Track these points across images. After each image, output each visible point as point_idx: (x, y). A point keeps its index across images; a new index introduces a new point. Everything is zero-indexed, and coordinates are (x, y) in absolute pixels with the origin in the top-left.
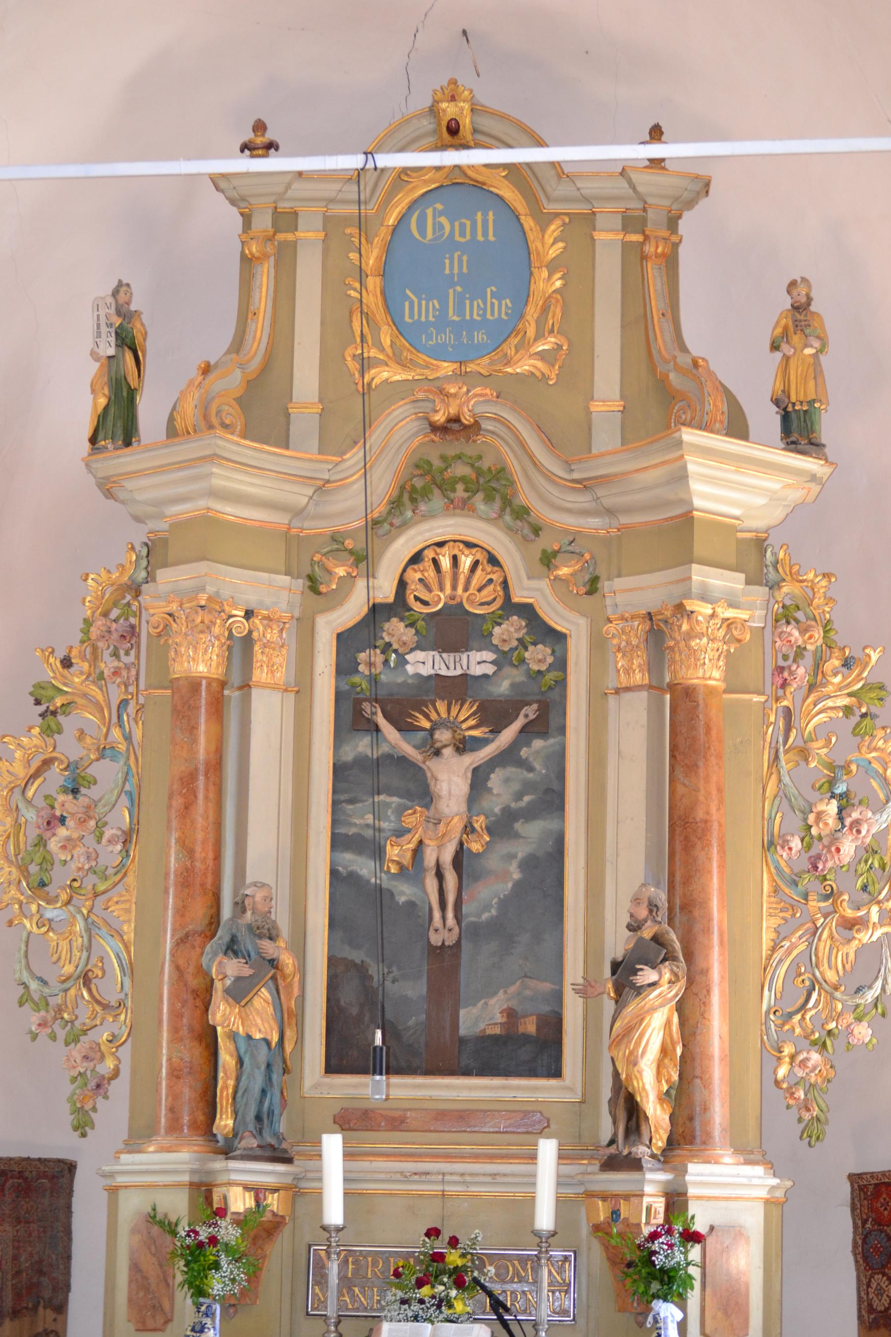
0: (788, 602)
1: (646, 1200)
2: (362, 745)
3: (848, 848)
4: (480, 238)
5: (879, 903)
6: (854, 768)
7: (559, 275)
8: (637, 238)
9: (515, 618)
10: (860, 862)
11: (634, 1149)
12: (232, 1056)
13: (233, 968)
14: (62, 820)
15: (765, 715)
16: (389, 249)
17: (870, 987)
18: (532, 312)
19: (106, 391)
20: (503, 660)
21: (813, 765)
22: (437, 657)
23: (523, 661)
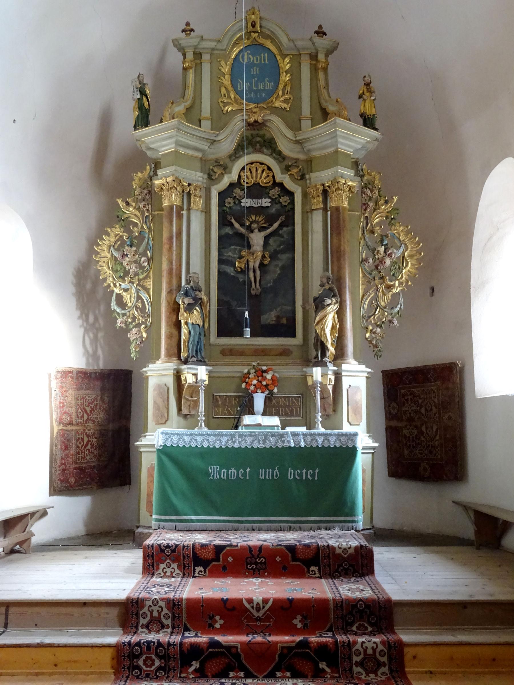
0: (366, 182)
1: (329, 377)
2: (228, 230)
3: (388, 261)
4: (263, 62)
5: (398, 280)
6: (389, 235)
7: (289, 75)
8: (314, 62)
9: (277, 188)
10: (392, 266)
11: (324, 359)
12: (187, 330)
13: (187, 301)
14: (127, 255)
15: (360, 219)
16: (233, 66)
17: (396, 307)
18: (281, 87)
19: (137, 110)
20: (274, 201)
21: (376, 235)
22: (251, 201)
23: (280, 202)
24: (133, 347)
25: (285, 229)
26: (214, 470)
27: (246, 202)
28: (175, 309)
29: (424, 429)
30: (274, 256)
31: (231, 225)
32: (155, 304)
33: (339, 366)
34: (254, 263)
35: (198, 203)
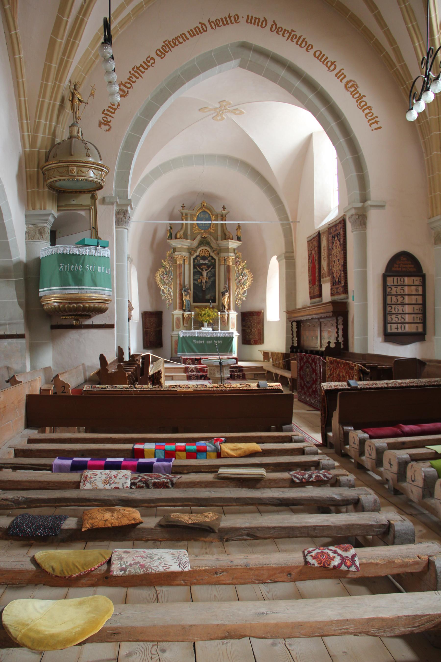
2: (195, 270)
3: (243, 281)
13: (185, 293)
20: (209, 261)
25: (213, 270)
28: (181, 295)
29: (252, 330)
30: (209, 278)
31: (197, 268)
32: (175, 293)
33: (229, 312)
34: (204, 281)
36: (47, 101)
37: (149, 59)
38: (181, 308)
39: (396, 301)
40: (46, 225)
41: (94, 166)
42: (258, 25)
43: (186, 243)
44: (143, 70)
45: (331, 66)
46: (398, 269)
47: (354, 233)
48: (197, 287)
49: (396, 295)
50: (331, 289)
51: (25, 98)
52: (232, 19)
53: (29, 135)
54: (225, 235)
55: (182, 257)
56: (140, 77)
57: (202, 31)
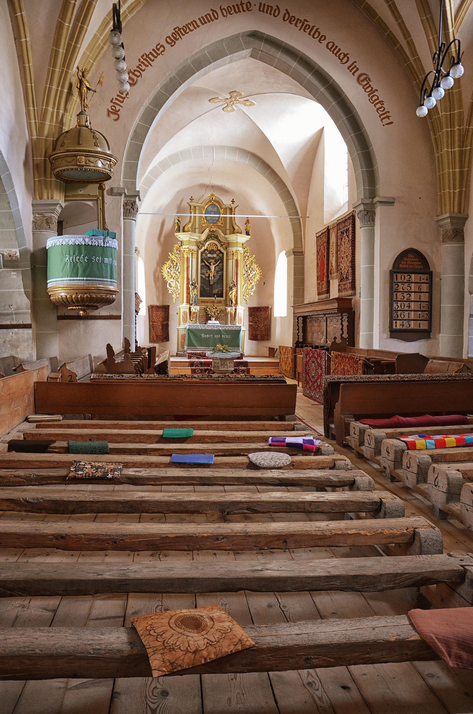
2: (203, 264)
3: (251, 275)
24: (174, 299)
26: (203, 335)
27: (209, 255)
28: (188, 288)
30: (217, 272)
31: (204, 262)
35: (195, 256)
36: (54, 87)
37: (158, 47)
38: (188, 302)
39: (402, 298)
40: (53, 215)
41: (103, 156)
42: (270, 14)
43: (196, 237)
44: (152, 58)
45: (343, 58)
46: (405, 266)
47: (362, 229)
48: (205, 281)
49: (403, 292)
50: (339, 285)
51: (31, 84)
52: (244, 6)
53: (36, 122)
54: (234, 229)
55: (189, 250)
56: (149, 65)
57: (213, 18)
